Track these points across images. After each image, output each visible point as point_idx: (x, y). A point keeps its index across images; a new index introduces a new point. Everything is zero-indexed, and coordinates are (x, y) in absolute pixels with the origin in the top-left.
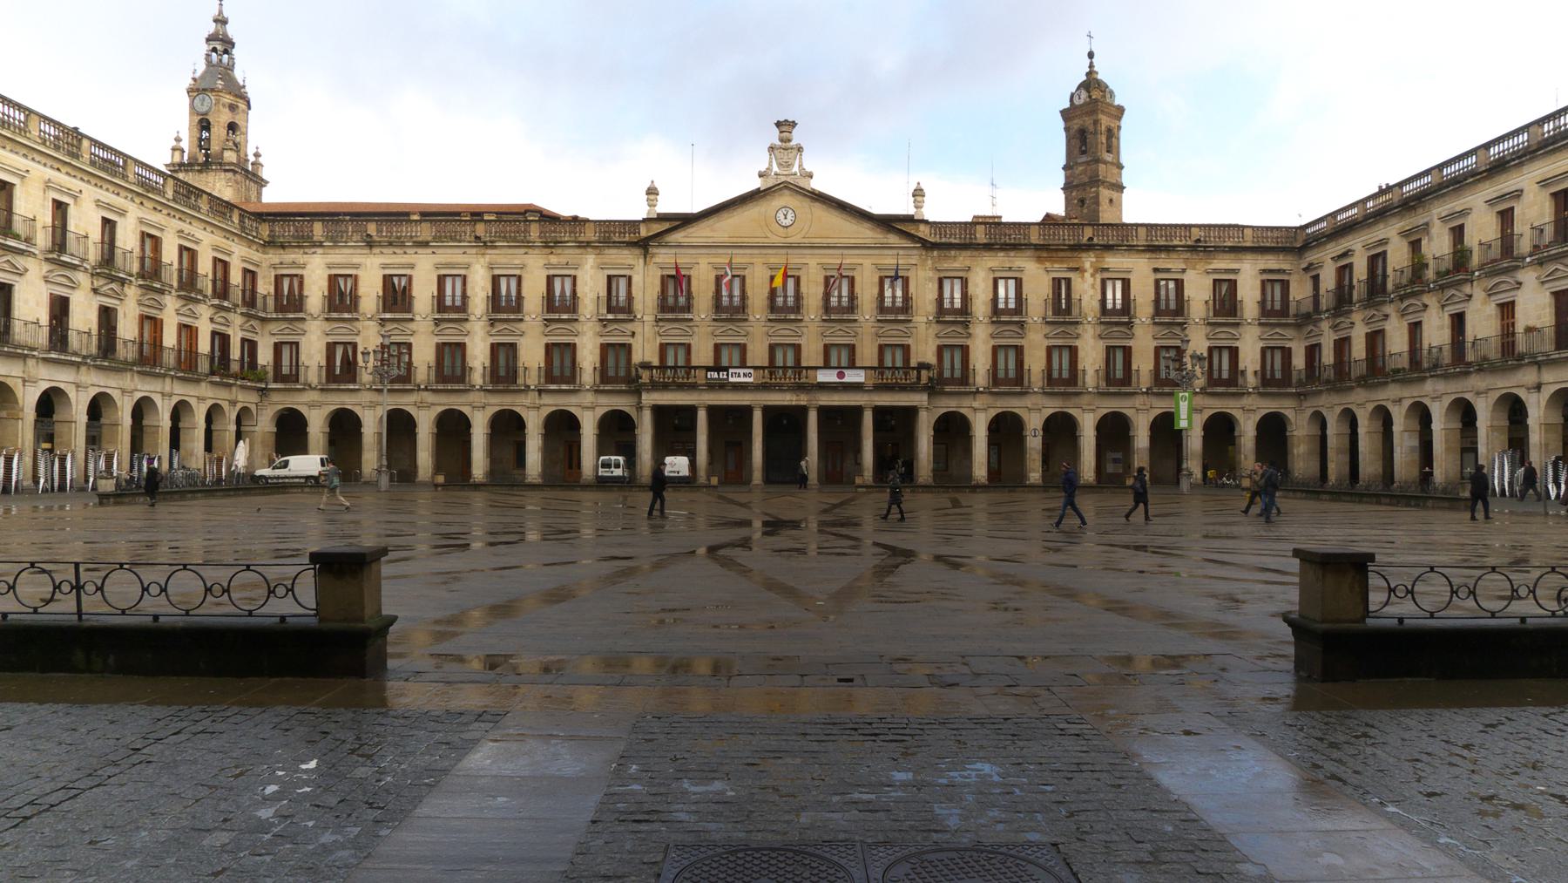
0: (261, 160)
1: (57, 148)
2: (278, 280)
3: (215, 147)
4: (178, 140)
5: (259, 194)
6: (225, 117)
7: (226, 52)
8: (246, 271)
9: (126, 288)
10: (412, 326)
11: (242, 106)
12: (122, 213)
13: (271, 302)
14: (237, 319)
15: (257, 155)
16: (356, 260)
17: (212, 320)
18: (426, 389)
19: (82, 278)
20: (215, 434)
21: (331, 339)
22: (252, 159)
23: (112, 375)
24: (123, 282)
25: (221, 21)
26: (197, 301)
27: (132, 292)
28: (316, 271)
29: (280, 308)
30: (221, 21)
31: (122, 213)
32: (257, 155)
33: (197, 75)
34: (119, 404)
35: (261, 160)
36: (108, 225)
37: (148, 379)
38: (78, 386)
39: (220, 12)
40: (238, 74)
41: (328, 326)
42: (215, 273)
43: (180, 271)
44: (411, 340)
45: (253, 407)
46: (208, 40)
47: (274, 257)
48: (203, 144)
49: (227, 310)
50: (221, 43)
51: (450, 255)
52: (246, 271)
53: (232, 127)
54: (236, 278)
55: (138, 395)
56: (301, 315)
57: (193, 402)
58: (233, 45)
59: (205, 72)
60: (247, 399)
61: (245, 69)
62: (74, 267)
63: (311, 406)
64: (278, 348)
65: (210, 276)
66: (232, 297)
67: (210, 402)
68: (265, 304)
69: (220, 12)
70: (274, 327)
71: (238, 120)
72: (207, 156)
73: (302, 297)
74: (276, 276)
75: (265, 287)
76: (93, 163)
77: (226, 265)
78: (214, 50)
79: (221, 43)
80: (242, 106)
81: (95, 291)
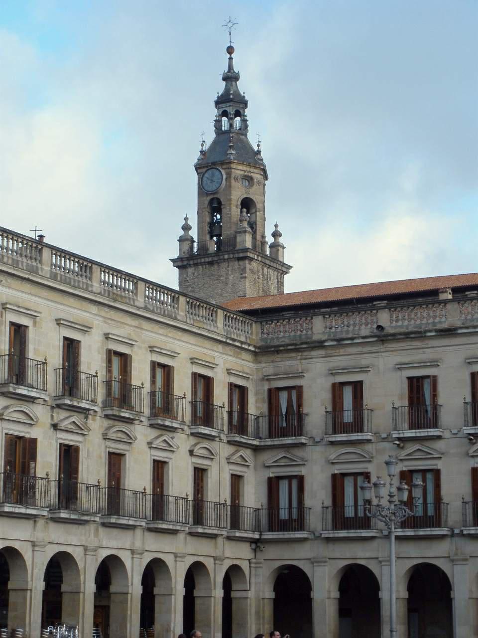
0: (281, 240)
1: (15, 264)
2: (273, 395)
3: (226, 233)
4: (186, 228)
5: (281, 284)
6: (238, 193)
7: (238, 114)
8: (232, 387)
9: (90, 421)
10: (439, 445)
11: (257, 176)
12: (85, 329)
13: (264, 424)
14: (223, 450)
15: (276, 235)
16: (365, 360)
17: (191, 453)
18: (462, 535)
19: (40, 412)
20: (198, 602)
21: (337, 470)
22: (270, 240)
23: (74, 528)
24: (85, 412)
25: (231, 77)
26: (172, 430)
27: (97, 425)
28: (316, 379)
29: (275, 431)
30: (231, 77)
31: (85, 329)
32: (276, 235)
33: (206, 147)
34: (81, 565)
35: (281, 240)
36: (71, 348)
37: (115, 532)
38: (34, 544)
39: (230, 67)
40: (252, 138)
41: (333, 453)
42: (194, 393)
43: (153, 394)
44: (439, 465)
45: (245, 566)
46: (218, 103)
47: (268, 367)
48: (213, 229)
49: (210, 438)
50: (231, 103)
51: (413, 355)
52: (232, 387)
53: (247, 204)
54: (220, 396)
55: (104, 554)
56: (303, 439)
57: (169, 560)
58: (245, 104)
59: (215, 143)
60: (241, 554)
61: (263, 130)
62: (32, 400)
63: (313, 562)
64: (273, 485)
65: (189, 397)
66: (217, 422)
67: (190, 561)
68: (258, 428)
69: (230, 67)
70: (269, 458)
71: (253, 194)
72: (218, 243)
73: (300, 416)
74: (270, 390)
75: (255, 407)
76: (54, 277)
77: (208, 382)
78: (225, 114)
79: (231, 103)
80: (257, 176)
81: (55, 427)
